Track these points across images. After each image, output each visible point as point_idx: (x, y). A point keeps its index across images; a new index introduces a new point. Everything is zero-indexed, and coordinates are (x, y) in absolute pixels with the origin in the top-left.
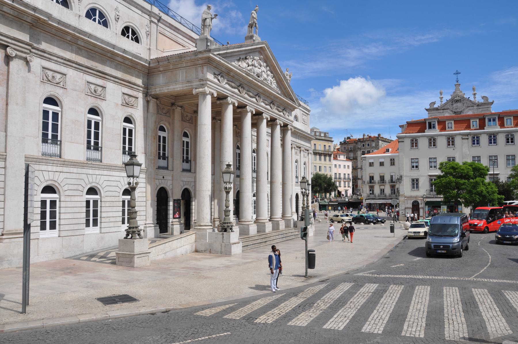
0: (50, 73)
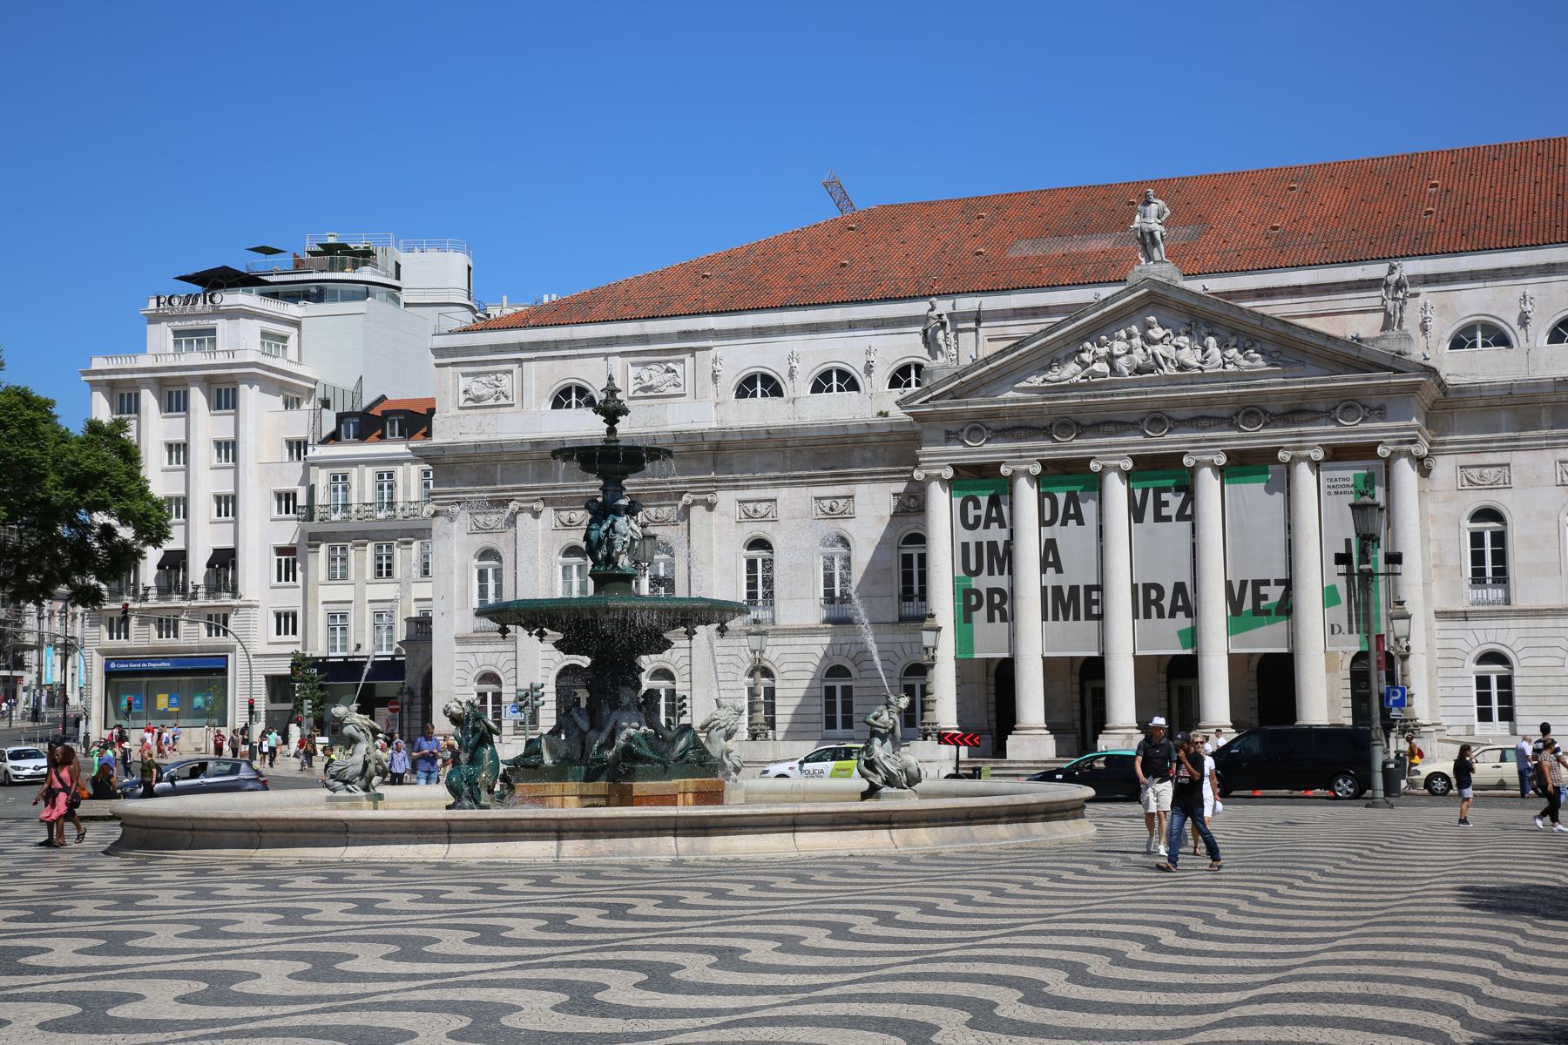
0: (751, 506)
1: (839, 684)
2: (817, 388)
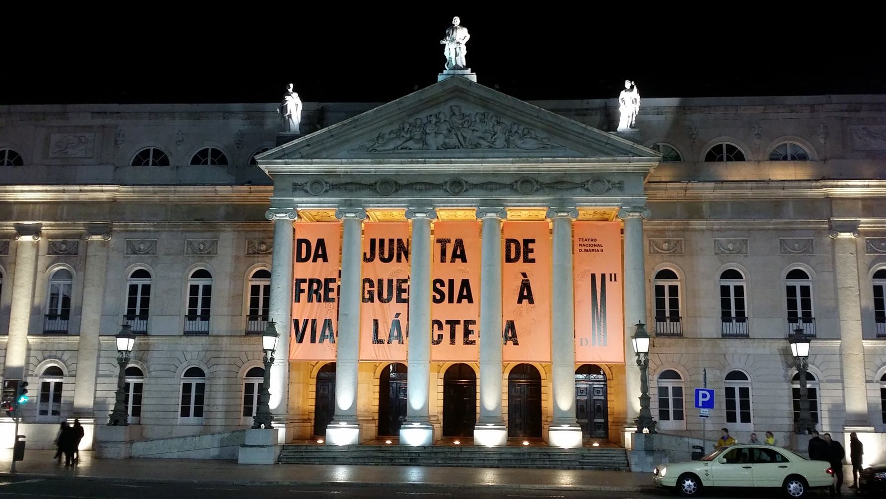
1: (194, 381)
2: (196, 161)
